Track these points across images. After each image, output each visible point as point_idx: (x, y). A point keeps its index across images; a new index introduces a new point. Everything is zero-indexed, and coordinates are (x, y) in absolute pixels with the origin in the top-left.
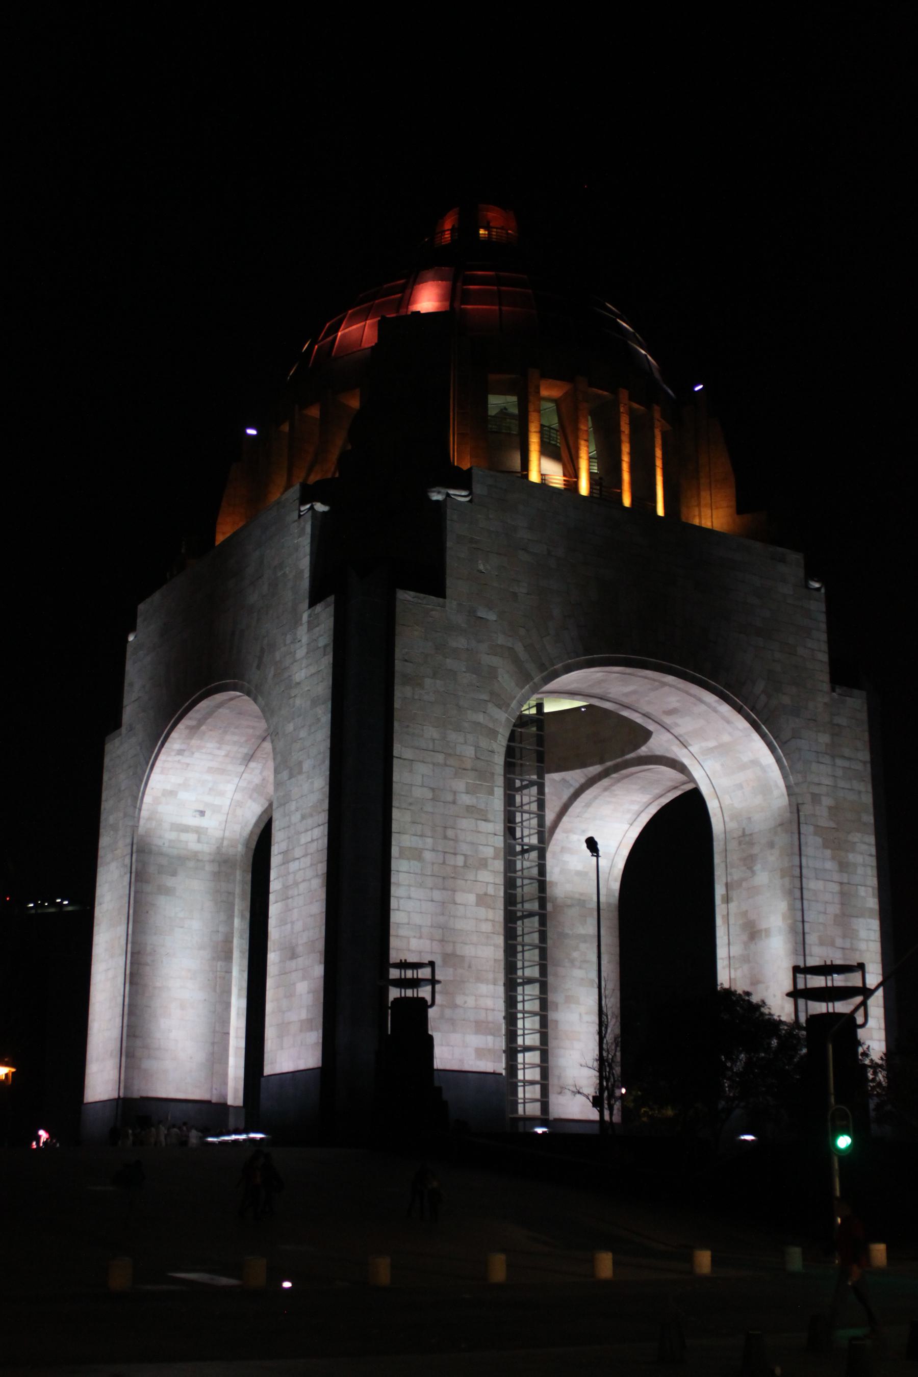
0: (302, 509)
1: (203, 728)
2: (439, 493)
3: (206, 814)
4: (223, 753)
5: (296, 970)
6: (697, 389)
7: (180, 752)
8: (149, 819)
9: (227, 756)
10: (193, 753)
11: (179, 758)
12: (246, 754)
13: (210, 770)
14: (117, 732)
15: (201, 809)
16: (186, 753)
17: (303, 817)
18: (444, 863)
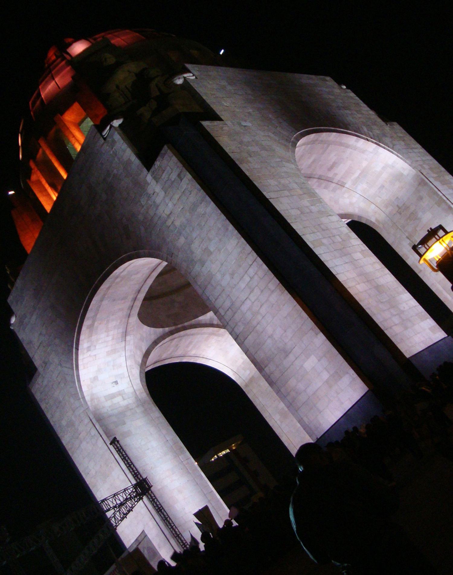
0: (104, 134)
1: (96, 324)
2: (179, 78)
3: (118, 382)
4: (110, 338)
5: (296, 358)
6: (221, 53)
7: (89, 349)
8: (92, 400)
9: (113, 339)
10: (95, 346)
11: (89, 353)
12: (123, 332)
13: (109, 354)
14: (37, 374)
15: (115, 380)
16: (92, 348)
17: (232, 275)
18: (334, 242)
